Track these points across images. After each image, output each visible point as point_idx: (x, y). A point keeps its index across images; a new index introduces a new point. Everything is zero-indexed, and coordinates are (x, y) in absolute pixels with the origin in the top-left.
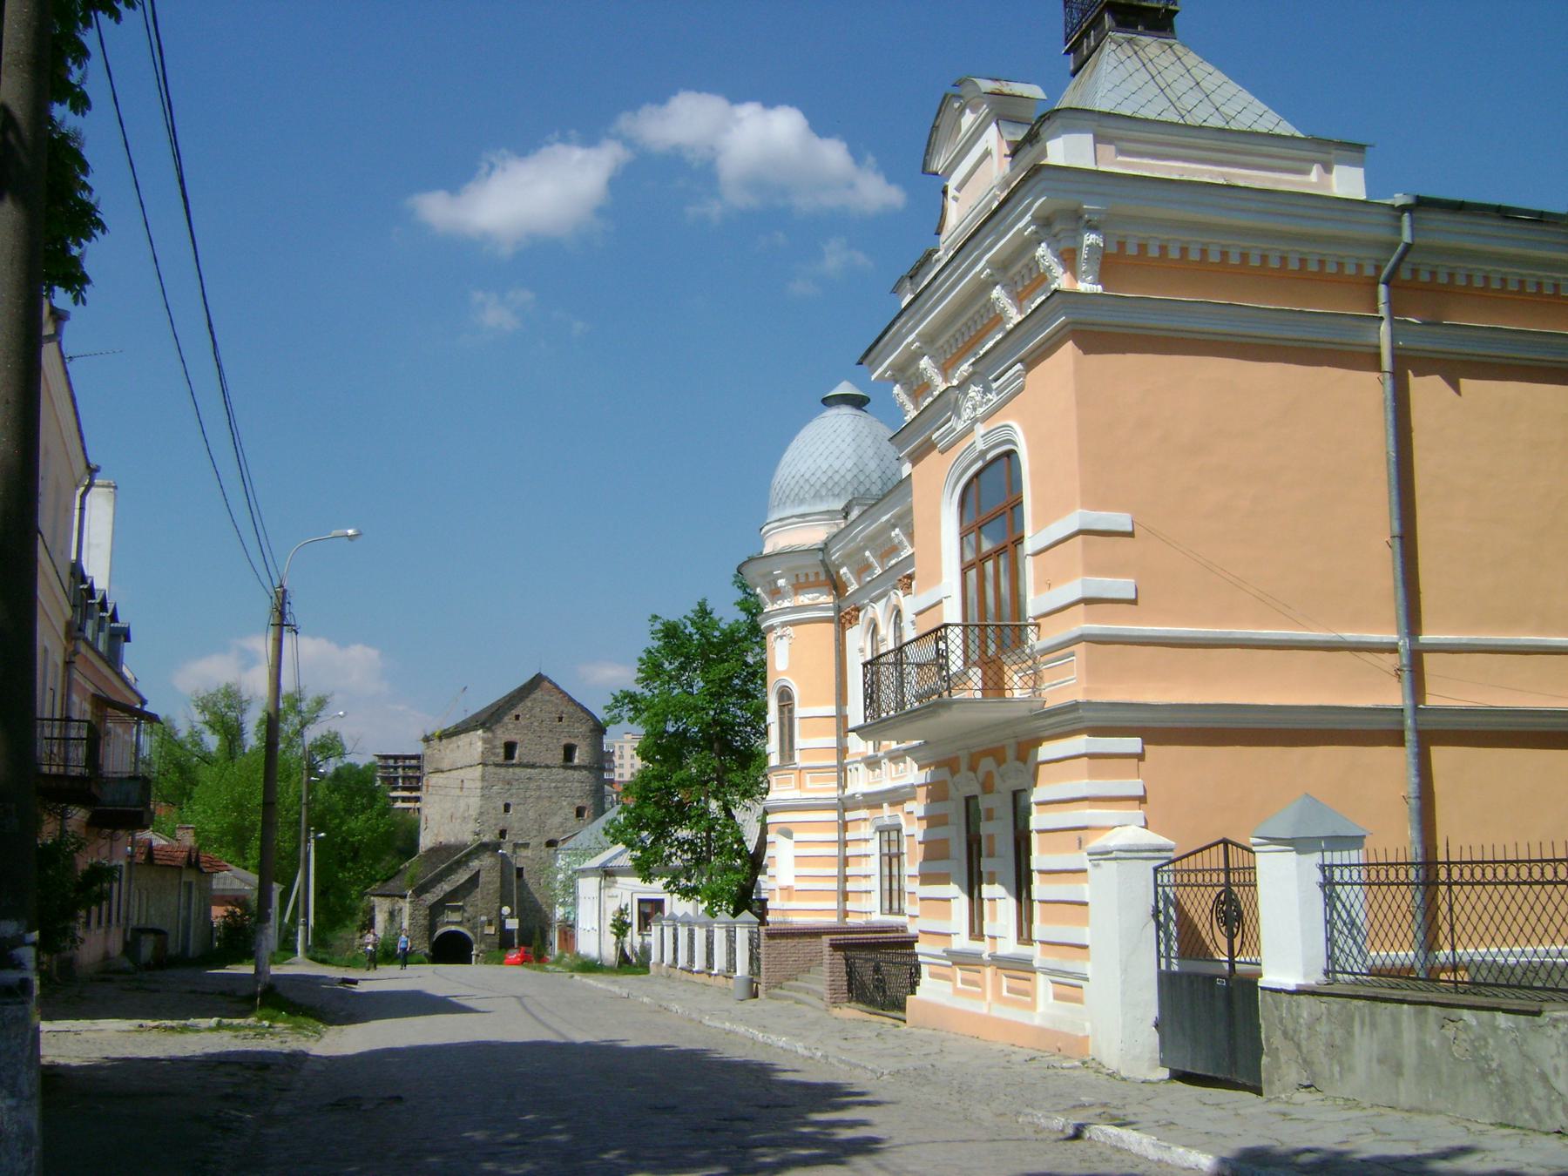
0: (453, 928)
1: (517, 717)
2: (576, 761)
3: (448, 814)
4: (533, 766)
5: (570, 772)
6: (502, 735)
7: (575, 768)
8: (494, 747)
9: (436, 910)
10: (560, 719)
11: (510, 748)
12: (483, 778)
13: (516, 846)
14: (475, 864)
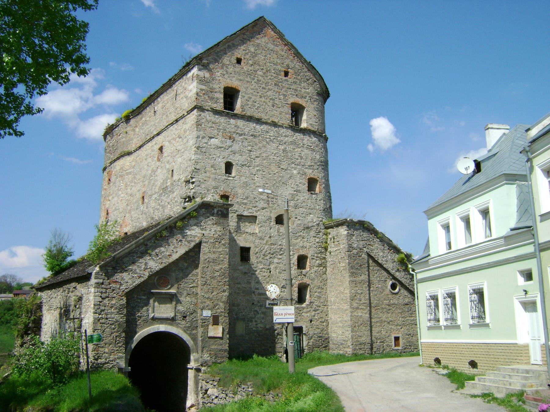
0: (162, 328)
1: (239, 61)
2: (304, 125)
3: (139, 196)
4: (259, 121)
5: (299, 136)
6: (225, 76)
7: (304, 131)
8: (212, 91)
9: (138, 297)
10: (286, 74)
11: (230, 96)
12: (198, 124)
13: (241, 218)
14: (194, 233)
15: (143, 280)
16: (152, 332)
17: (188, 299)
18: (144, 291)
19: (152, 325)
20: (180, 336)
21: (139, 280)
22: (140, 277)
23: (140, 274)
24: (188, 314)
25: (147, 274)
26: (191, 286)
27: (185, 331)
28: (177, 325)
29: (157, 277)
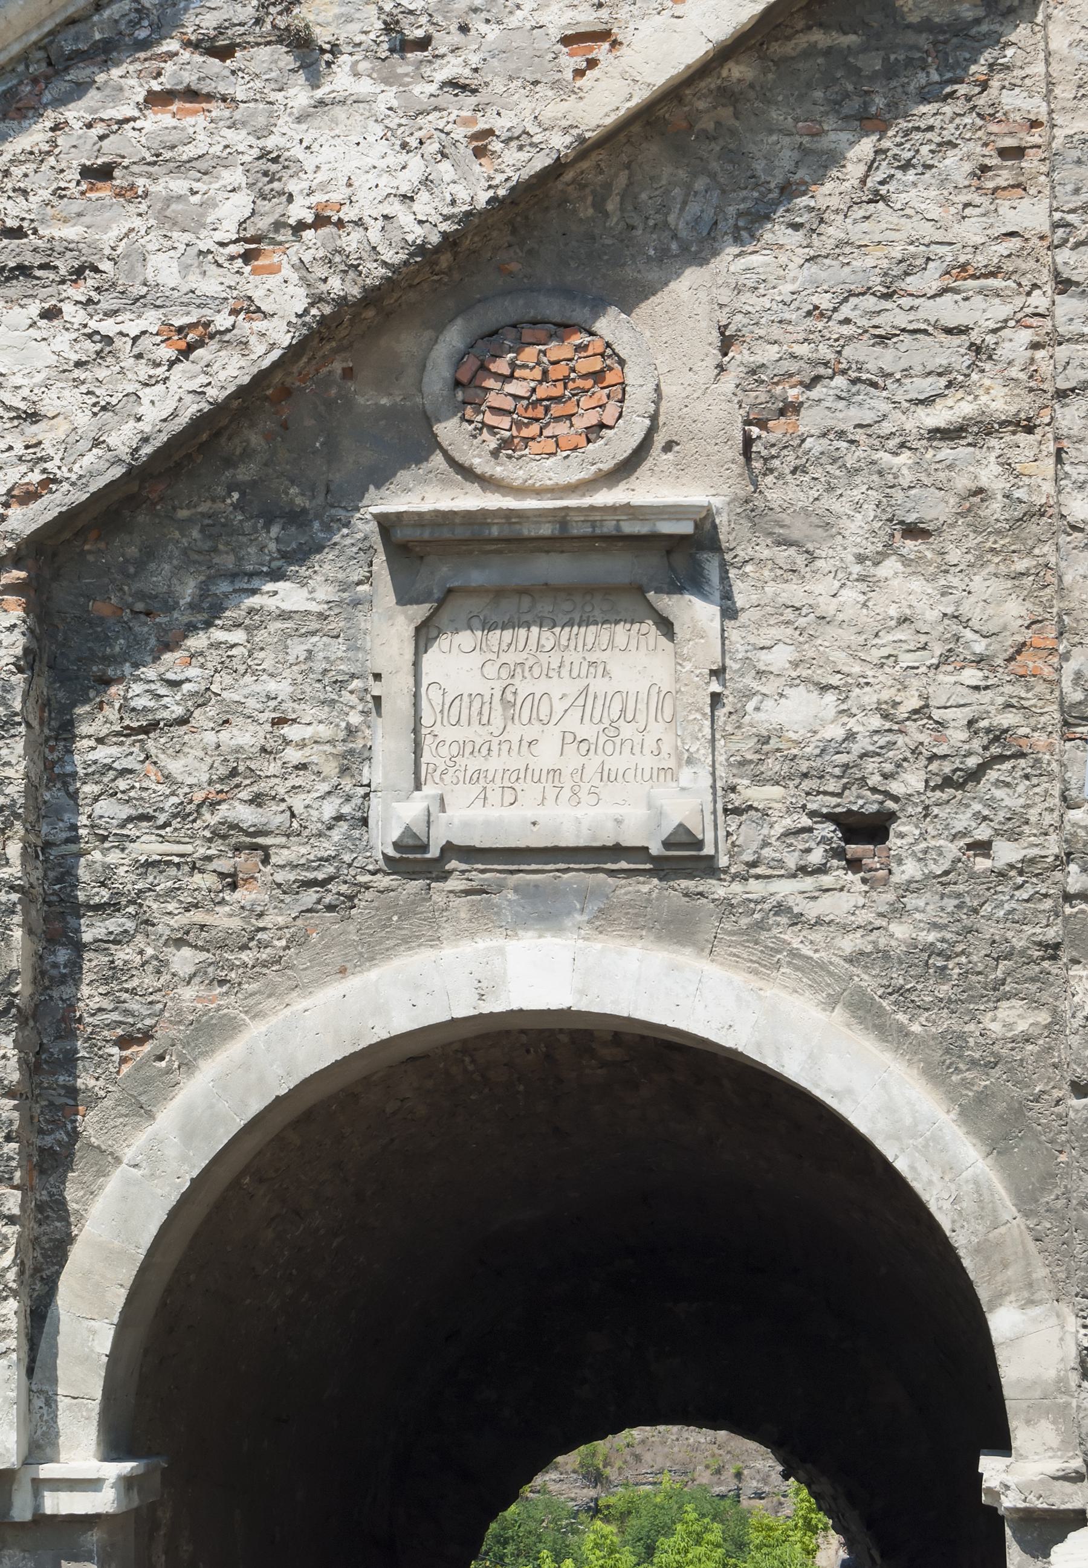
15: (228, 371)
16: (402, 1022)
17: (904, 587)
18: (296, 518)
19: (408, 942)
20: (793, 1067)
21: (184, 378)
22: (190, 340)
23: (194, 299)
24: (911, 781)
25: (284, 301)
26: (939, 416)
27: (864, 1011)
28: (759, 936)
29: (453, 338)
